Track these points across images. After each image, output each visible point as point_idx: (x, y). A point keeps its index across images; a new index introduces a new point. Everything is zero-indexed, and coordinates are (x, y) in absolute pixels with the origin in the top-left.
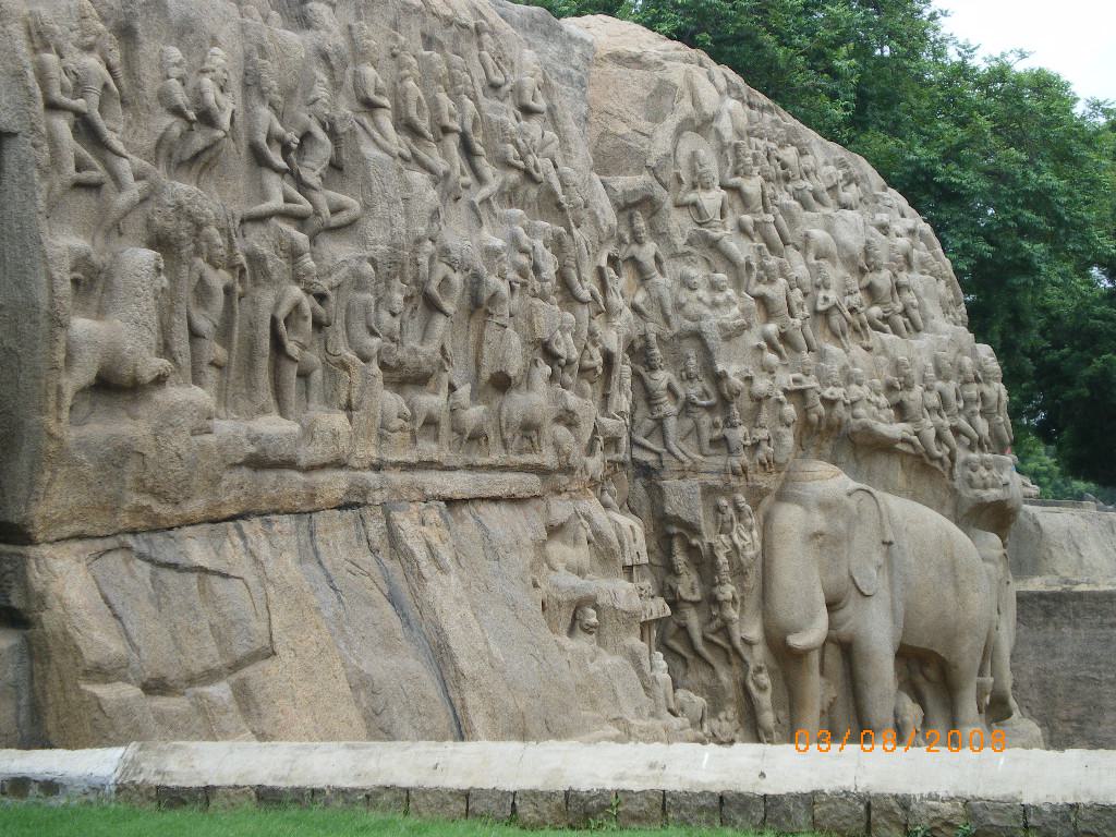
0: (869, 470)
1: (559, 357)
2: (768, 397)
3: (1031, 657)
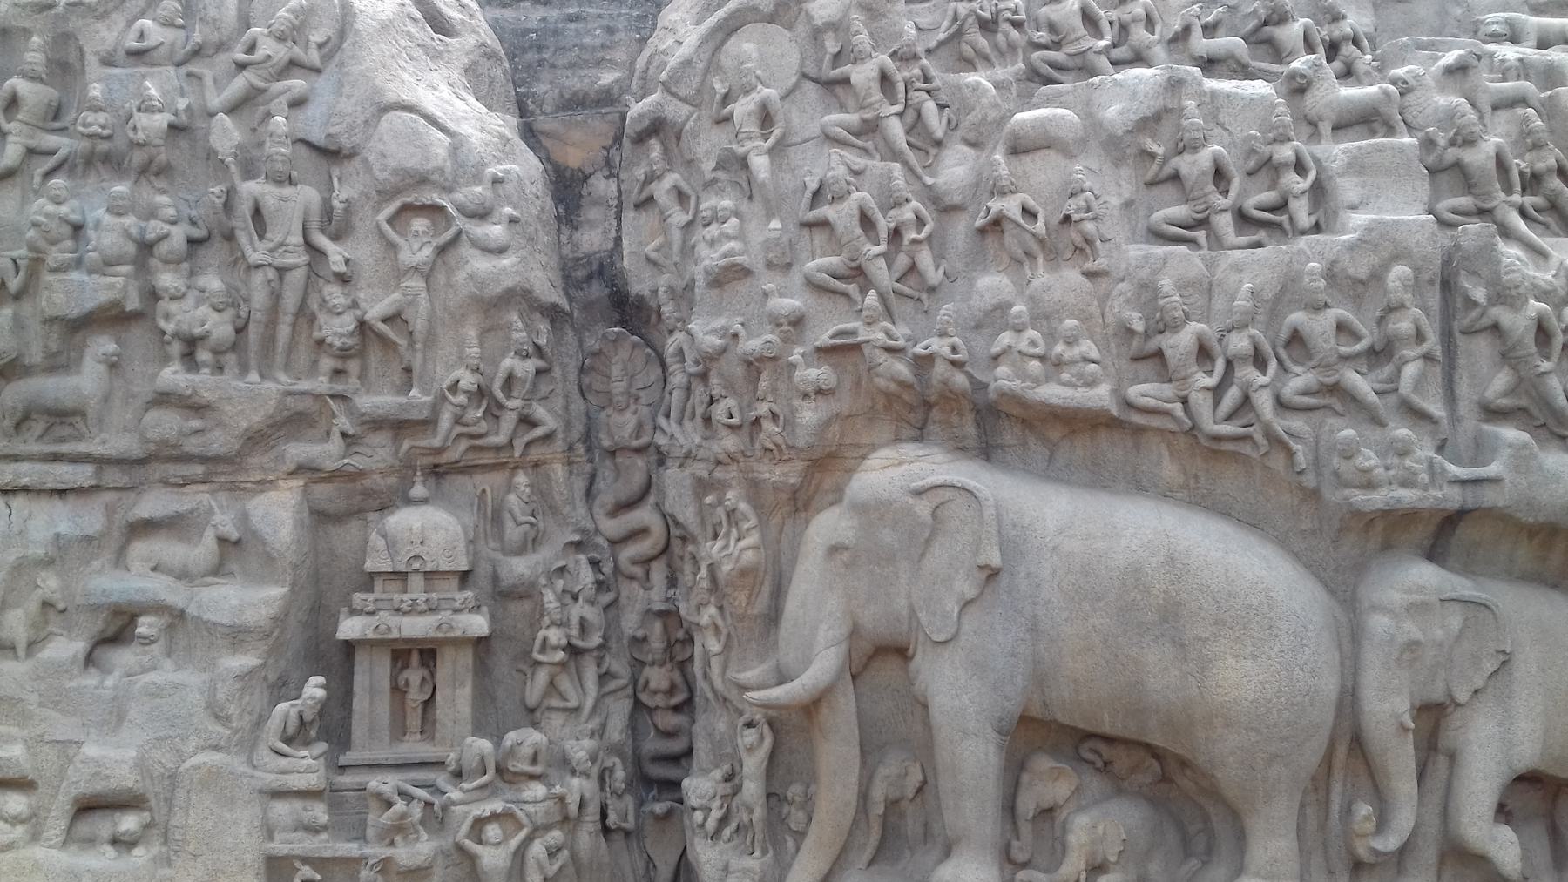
1: (164, 333)
2: (761, 359)
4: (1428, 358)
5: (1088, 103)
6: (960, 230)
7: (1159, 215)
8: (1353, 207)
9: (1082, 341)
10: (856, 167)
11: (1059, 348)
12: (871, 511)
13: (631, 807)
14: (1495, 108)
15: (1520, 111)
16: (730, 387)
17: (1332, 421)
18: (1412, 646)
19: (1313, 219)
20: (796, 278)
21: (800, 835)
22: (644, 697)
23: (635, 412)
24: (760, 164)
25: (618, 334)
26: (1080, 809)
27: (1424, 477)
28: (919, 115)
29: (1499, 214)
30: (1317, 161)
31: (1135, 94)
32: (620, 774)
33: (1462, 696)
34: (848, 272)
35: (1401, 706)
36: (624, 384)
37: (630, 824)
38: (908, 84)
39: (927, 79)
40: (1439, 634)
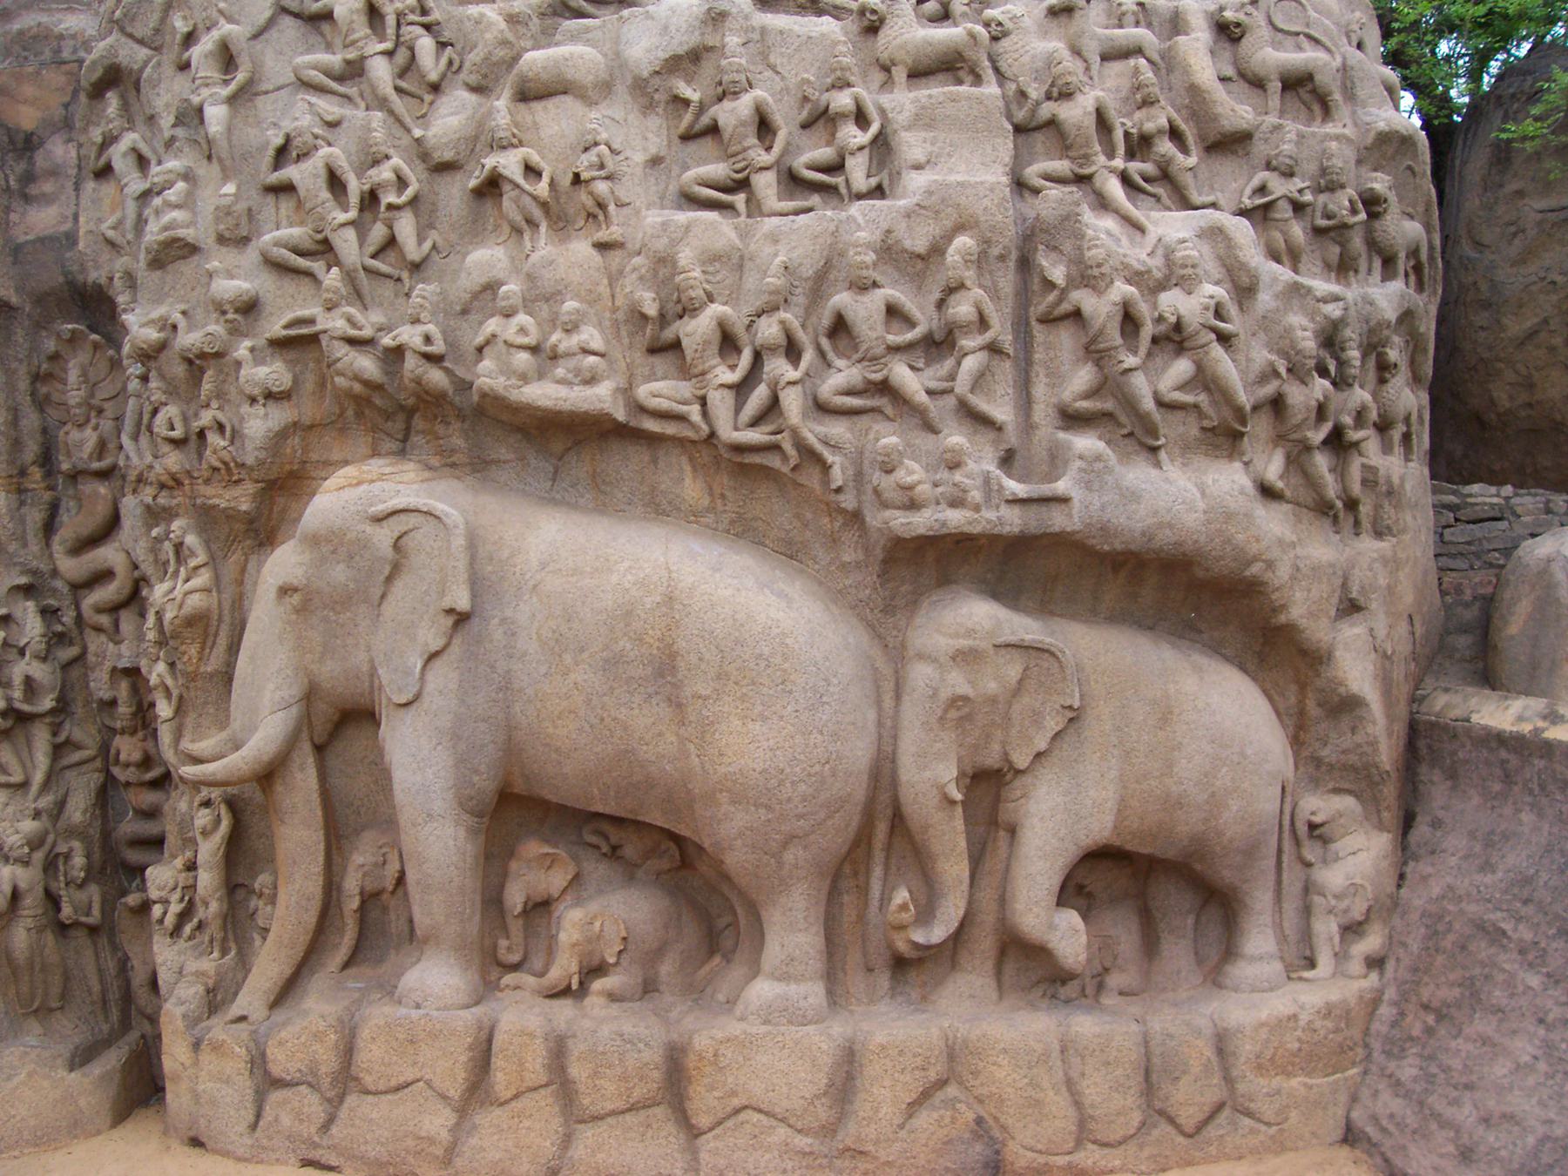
0: (594, 476)
2: (203, 355)
3: (1453, 861)
4: (993, 349)
5: (617, 40)
6: (454, 193)
7: (691, 174)
8: (918, 167)
9: (583, 328)
10: (329, 118)
11: (554, 338)
12: (327, 543)
13: (97, 899)
14: (1105, 58)
15: (1132, 62)
16: (172, 391)
17: (880, 426)
18: (956, 701)
19: (873, 181)
20: (251, 255)
21: (265, 931)
22: (116, 771)
23: (95, 428)
24: (216, 115)
25: (73, 332)
26: (579, 902)
27: (976, 495)
28: (413, 56)
29: (1097, 181)
30: (882, 112)
31: (666, 28)
32: (79, 860)
33: (1021, 760)
34: (314, 247)
35: (947, 772)
36: (82, 393)
37: (95, 917)
38: (400, 16)
39: (424, 12)
40: (992, 687)
